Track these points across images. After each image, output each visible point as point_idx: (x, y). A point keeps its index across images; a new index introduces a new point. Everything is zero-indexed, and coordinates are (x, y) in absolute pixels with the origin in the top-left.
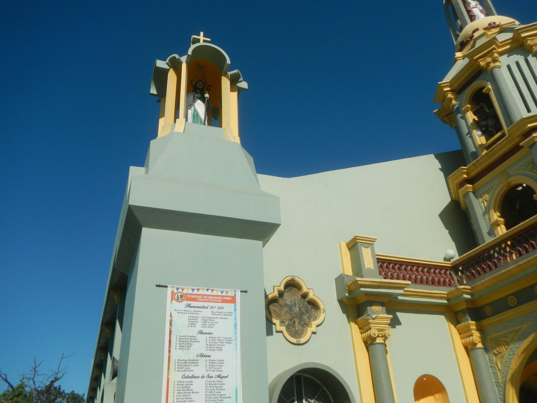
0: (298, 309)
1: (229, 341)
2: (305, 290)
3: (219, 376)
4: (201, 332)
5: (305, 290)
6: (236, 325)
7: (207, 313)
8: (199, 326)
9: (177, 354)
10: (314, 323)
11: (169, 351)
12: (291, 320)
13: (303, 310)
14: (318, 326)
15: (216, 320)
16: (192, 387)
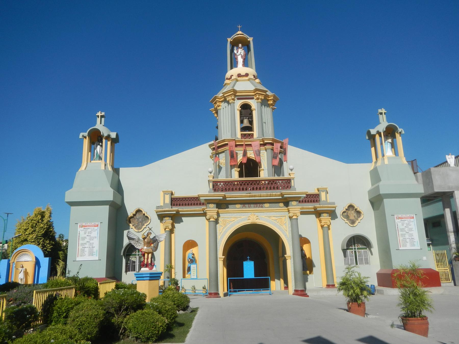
0: (141, 220)
1: (96, 237)
2: (143, 213)
3: (92, 247)
4: (88, 236)
5: (143, 213)
6: (98, 233)
7: (89, 230)
8: (87, 234)
9: (81, 242)
10: (145, 224)
11: (79, 241)
12: (138, 224)
13: (143, 220)
15: (92, 232)
16: (85, 250)
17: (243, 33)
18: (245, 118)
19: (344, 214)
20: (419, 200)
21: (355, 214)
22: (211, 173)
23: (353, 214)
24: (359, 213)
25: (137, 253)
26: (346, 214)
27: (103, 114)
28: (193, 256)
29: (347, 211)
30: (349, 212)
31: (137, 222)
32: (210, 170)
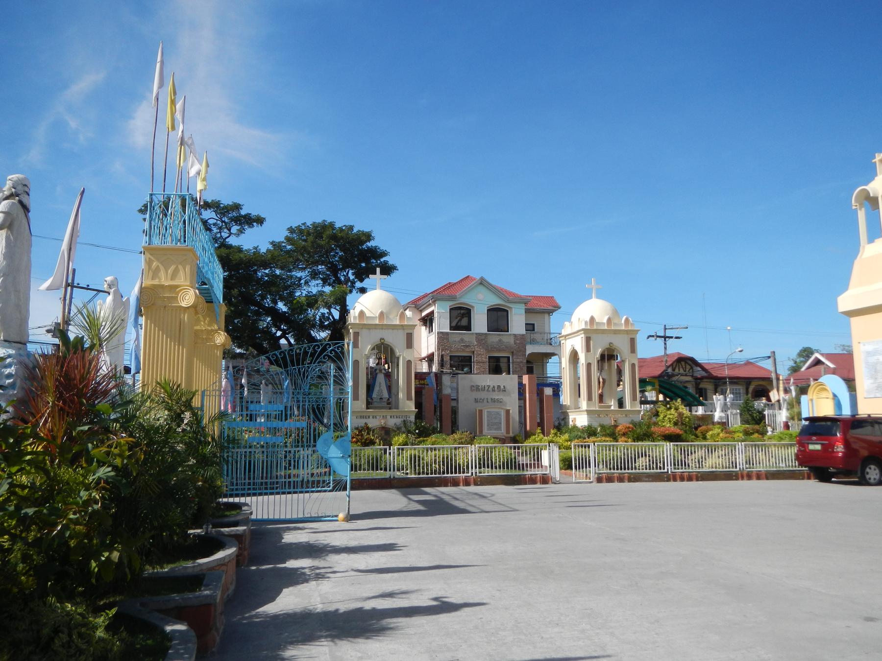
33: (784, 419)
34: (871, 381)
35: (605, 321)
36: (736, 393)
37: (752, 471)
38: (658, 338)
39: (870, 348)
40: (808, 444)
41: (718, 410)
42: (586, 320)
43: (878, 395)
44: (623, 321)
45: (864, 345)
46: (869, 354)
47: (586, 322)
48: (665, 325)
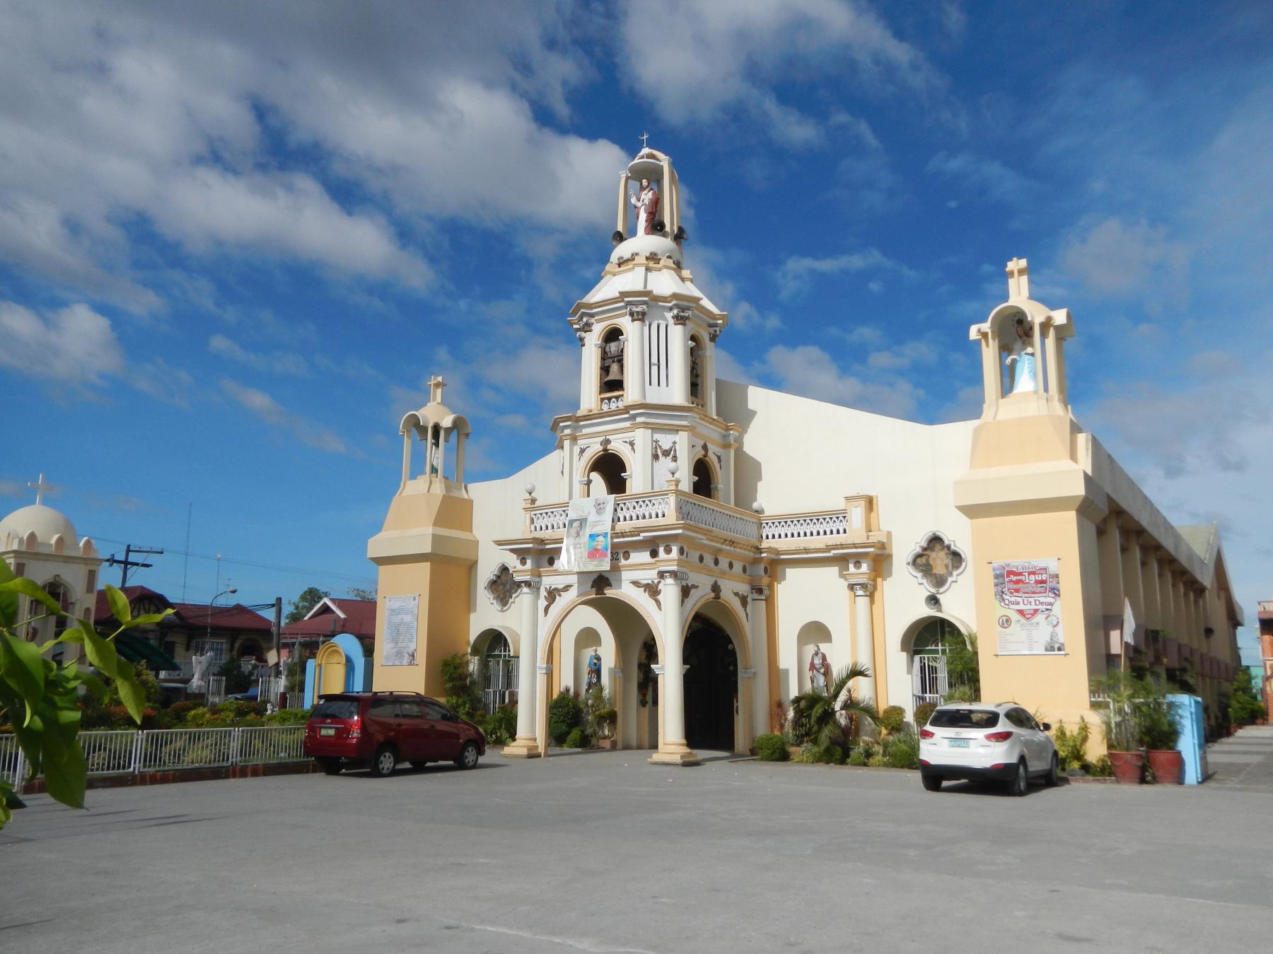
10: (514, 596)
14: (515, 597)
17: (650, 150)
18: (613, 362)
19: (919, 561)
20: (1072, 515)
21: (948, 561)
22: (530, 493)
23: (942, 560)
24: (956, 557)
25: (503, 653)
26: (923, 560)
27: (440, 379)
28: (595, 661)
29: (925, 553)
30: (933, 555)
31: (503, 591)
32: (529, 487)
33: (282, 690)
34: (392, 645)
35: (53, 541)
36: (217, 649)
37: (247, 766)
38: (115, 564)
39: (395, 604)
40: (321, 728)
41: (196, 677)
42: (21, 536)
43: (397, 663)
44: (81, 545)
45: (390, 601)
46: (393, 610)
47: (21, 541)
48: (129, 546)
